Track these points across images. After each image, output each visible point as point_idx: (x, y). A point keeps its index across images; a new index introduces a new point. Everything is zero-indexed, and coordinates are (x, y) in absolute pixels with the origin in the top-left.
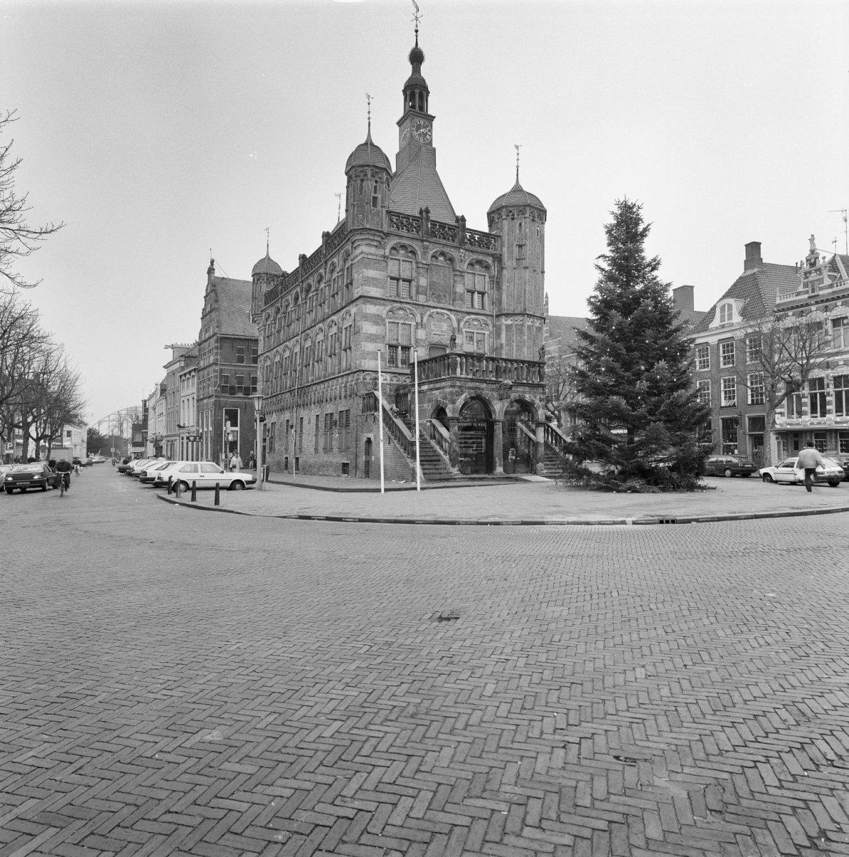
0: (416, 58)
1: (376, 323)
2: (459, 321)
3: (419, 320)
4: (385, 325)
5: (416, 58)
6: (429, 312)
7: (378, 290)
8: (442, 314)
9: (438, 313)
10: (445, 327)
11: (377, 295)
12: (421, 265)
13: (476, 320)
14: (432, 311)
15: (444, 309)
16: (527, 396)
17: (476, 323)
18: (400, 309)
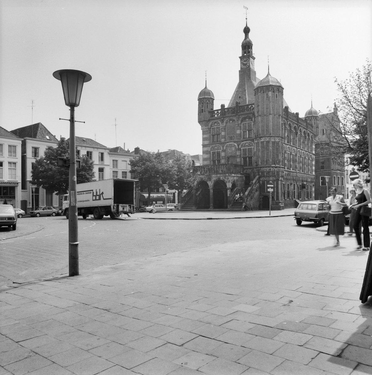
0: (247, 31)
1: (207, 154)
2: (238, 146)
3: (222, 149)
4: (210, 154)
5: (247, 31)
6: (226, 145)
7: (207, 141)
8: (232, 144)
9: (230, 144)
10: (233, 149)
11: (207, 143)
12: (222, 127)
13: (247, 143)
14: (227, 144)
15: (231, 142)
16: (221, 178)
17: (247, 144)
18: (215, 146)
